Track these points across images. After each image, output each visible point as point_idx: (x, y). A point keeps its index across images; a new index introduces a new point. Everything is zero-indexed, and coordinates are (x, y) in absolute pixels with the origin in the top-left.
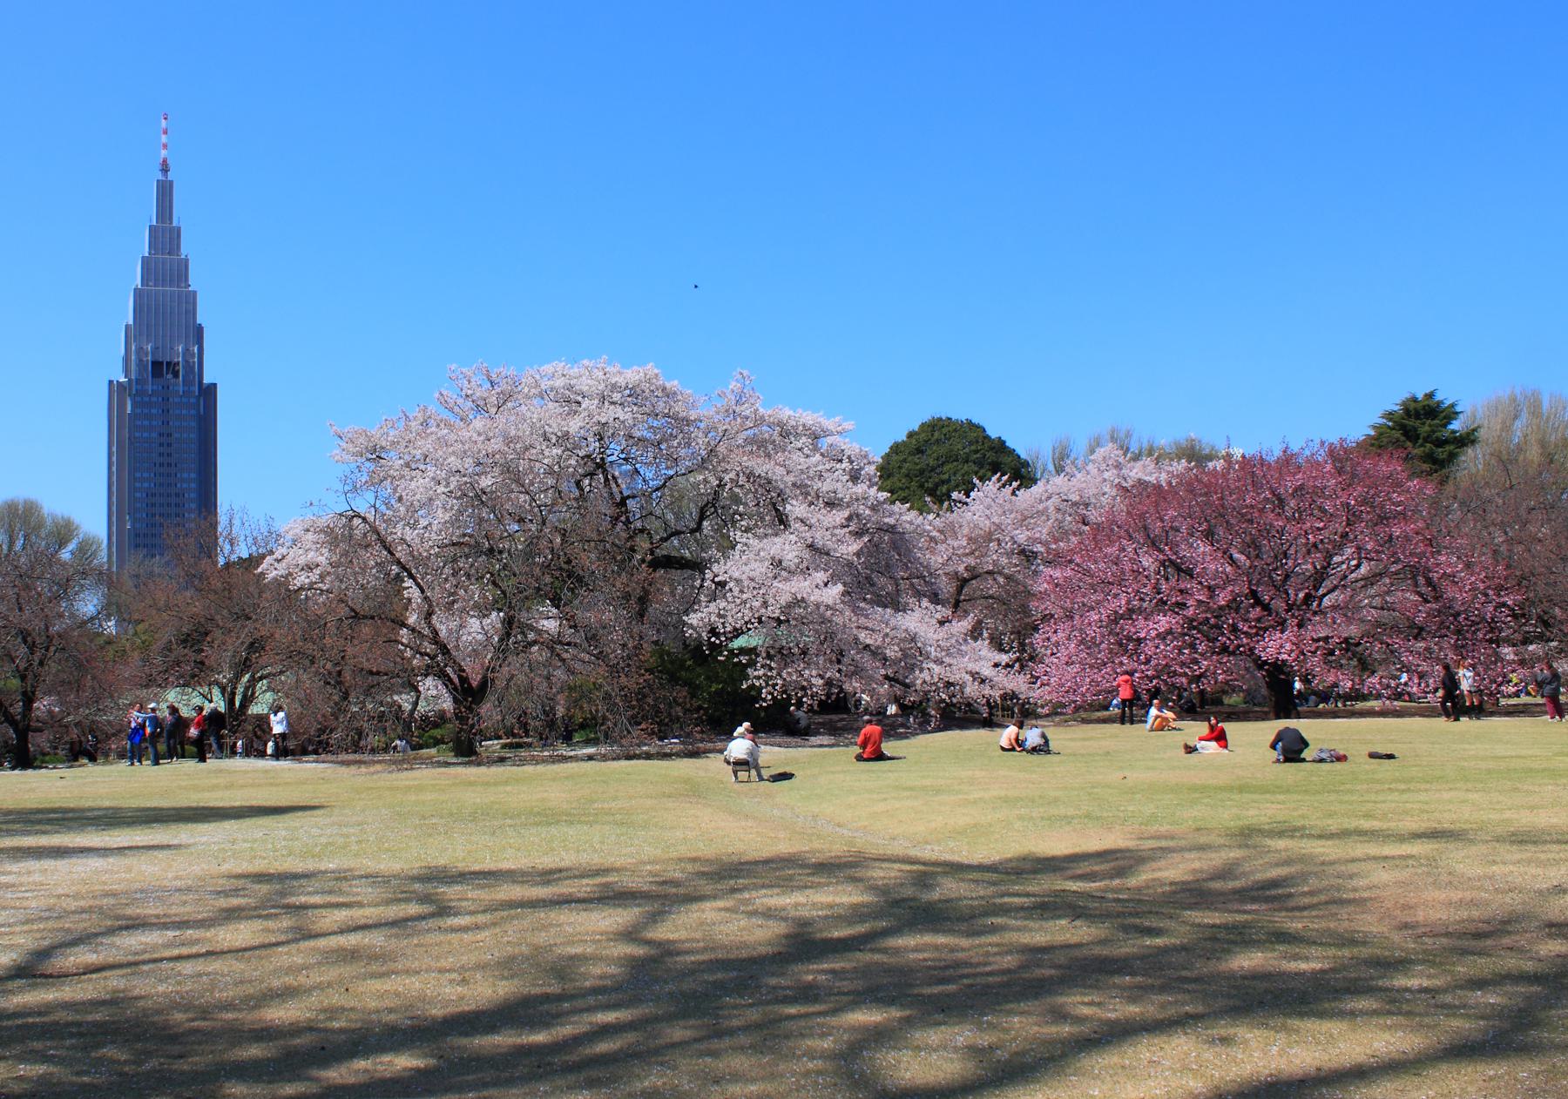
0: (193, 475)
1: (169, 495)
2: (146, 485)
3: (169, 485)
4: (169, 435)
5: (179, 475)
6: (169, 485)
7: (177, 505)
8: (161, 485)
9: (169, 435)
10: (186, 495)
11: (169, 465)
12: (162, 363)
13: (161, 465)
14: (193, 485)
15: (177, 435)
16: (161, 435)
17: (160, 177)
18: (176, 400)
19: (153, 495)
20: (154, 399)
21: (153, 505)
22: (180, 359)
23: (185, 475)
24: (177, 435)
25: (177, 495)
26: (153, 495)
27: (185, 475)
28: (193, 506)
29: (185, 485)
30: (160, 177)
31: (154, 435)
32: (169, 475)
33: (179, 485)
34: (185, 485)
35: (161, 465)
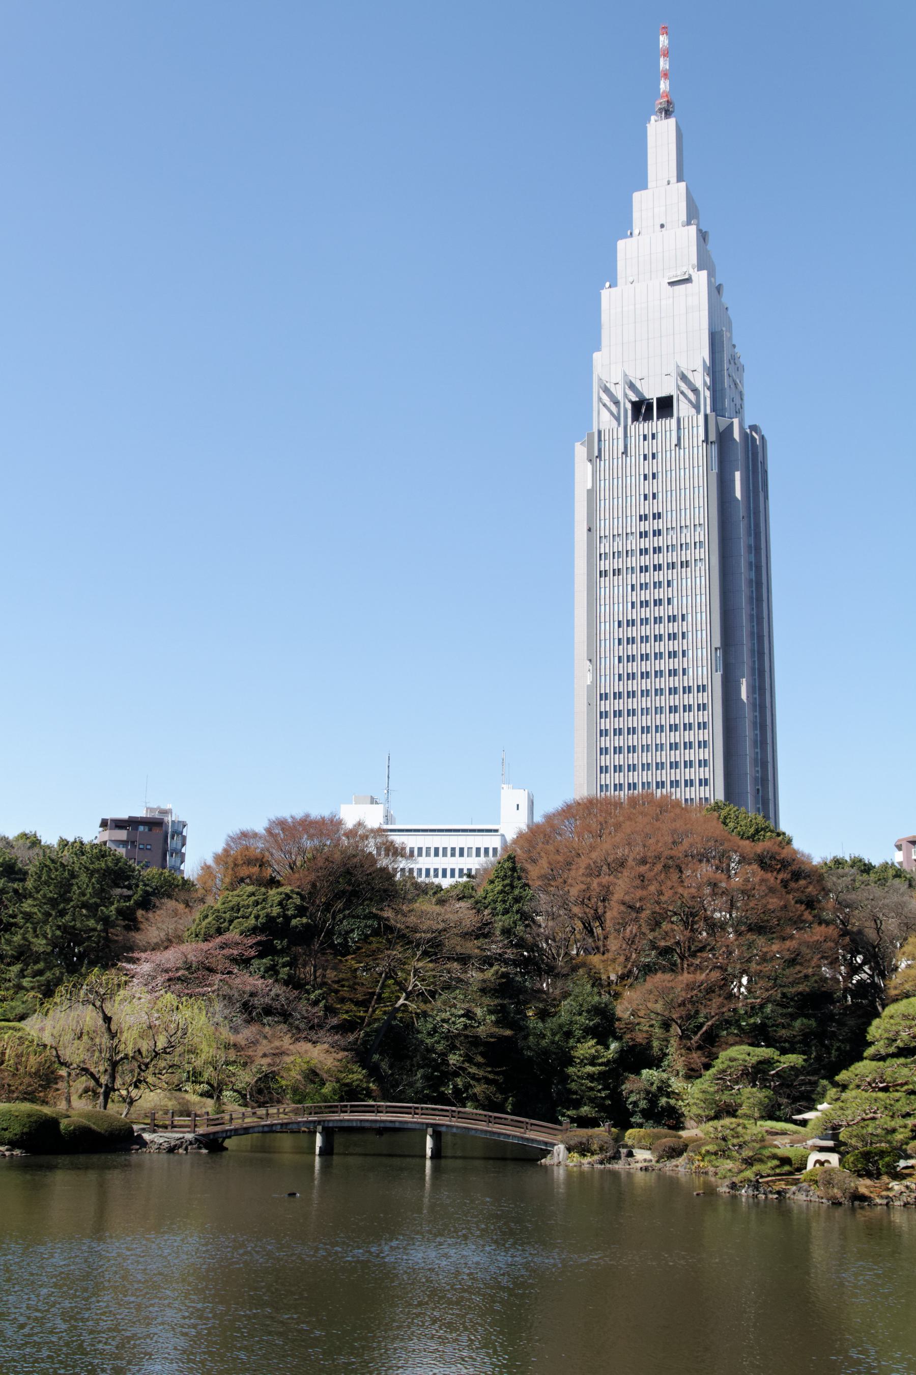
25: (672, 619)
32: (658, 585)
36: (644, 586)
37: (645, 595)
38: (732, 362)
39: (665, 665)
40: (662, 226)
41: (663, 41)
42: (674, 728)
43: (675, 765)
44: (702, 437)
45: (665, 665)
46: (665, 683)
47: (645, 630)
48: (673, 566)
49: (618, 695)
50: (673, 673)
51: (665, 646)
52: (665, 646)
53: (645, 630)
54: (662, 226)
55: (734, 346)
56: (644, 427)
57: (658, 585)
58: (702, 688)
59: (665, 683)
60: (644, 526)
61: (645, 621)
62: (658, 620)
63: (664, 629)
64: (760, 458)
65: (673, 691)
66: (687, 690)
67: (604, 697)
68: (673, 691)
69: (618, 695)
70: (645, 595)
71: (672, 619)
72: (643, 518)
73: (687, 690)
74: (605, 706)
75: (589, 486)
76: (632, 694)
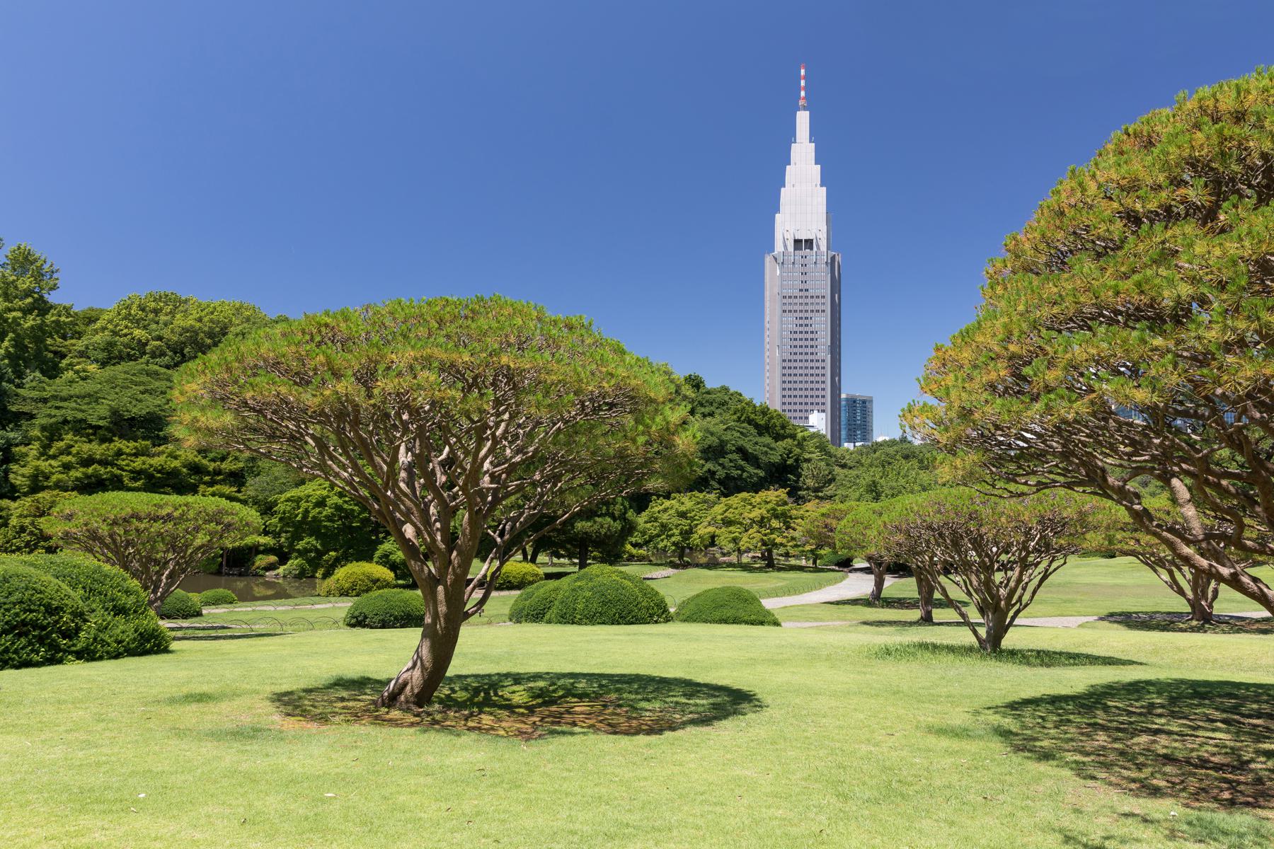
3: (807, 325)
4: (807, 290)
19: (796, 332)
25: (812, 332)
26: (796, 332)
37: (801, 322)
39: (809, 350)
41: (803, 72)
42: (812, 375)
43: (812, 389)
45: (809, 350)
46: (809, 357)
47: (801, 336)
48: (812, 311)
49: (790, 361)
50: (812, 354)
51: (809, 343)
52: (809, 343)
53: (801, 336)
57: (807, 318)
59: (809, 357)
60: (801, 294)
61: (801, 332)
62: (807, 332)
63: (809, 336)
65: (812, 361)
66: (818, 361)
68: (812, 361)
69: (790, 361)
70: (801, 322)
71: (812, 332)
72: (801, 290)
73: (818, 361)
74: (785, 364)
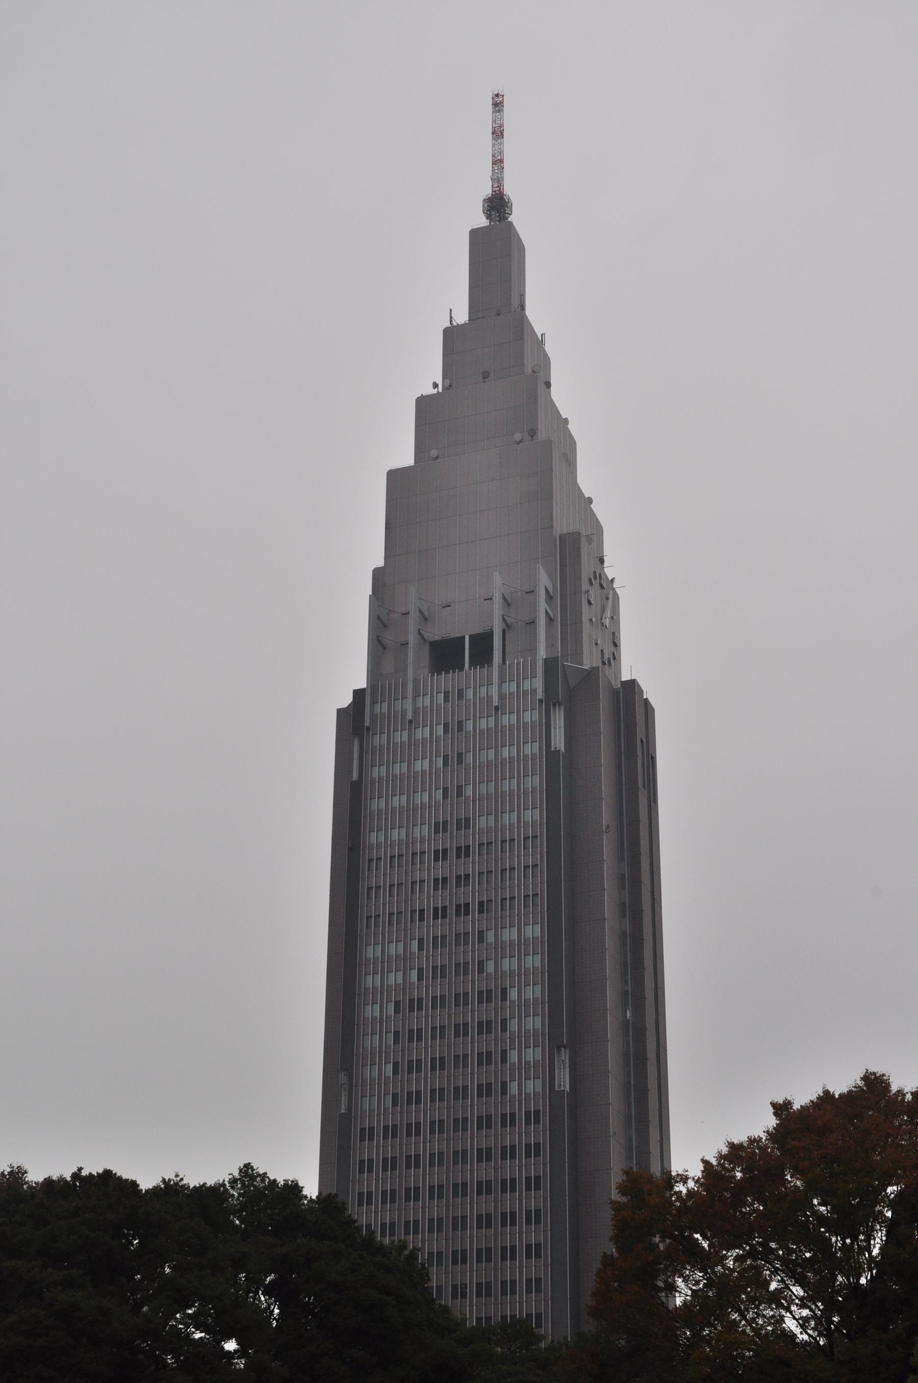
0: (533, 931)
1: (461, 999)
2: (396, 978)
3: (462, 968)
5: (490, 937)
6: (462, 968)
7: (485, 1027)
8: (440, 971)
9: (464, 824)
10: (513, 994)
11: (463, 910)
12: (463, 638)
13: (440, 913)
14: (534, 961)
15: (483, 822)
16: (440, 827)
17: (482, 221)
18: (483, 724)
20: (422, 733)
21: (415, 1035)
22: (560, 655)
23: (510, 934)
24: (483, 822)
25: (485, 996)
26: (416, 1005)
27: (510, 934)
28: (534, 1023)
29: (506, 965)
30: (482, 221)
31: (422, 831)
32: (462, 938)
33: (490, 967)
34: (506, 965)
35: (440, 913)
36: (439, 942)
38: (596, 583)
40: (485, 375)
44: (540, 694)
54: (485, 375)
55: (602, 561)
56: (448, 680)
57: (462, 938)
58: (533, 1117)
63: (473, 1014)
64: (640, 733)
66: (509, 1120)
67: (368, 1134)
69: (391, 1132)
73: (509, 1120)
75: (355, 776)
76: (414, 1130)
